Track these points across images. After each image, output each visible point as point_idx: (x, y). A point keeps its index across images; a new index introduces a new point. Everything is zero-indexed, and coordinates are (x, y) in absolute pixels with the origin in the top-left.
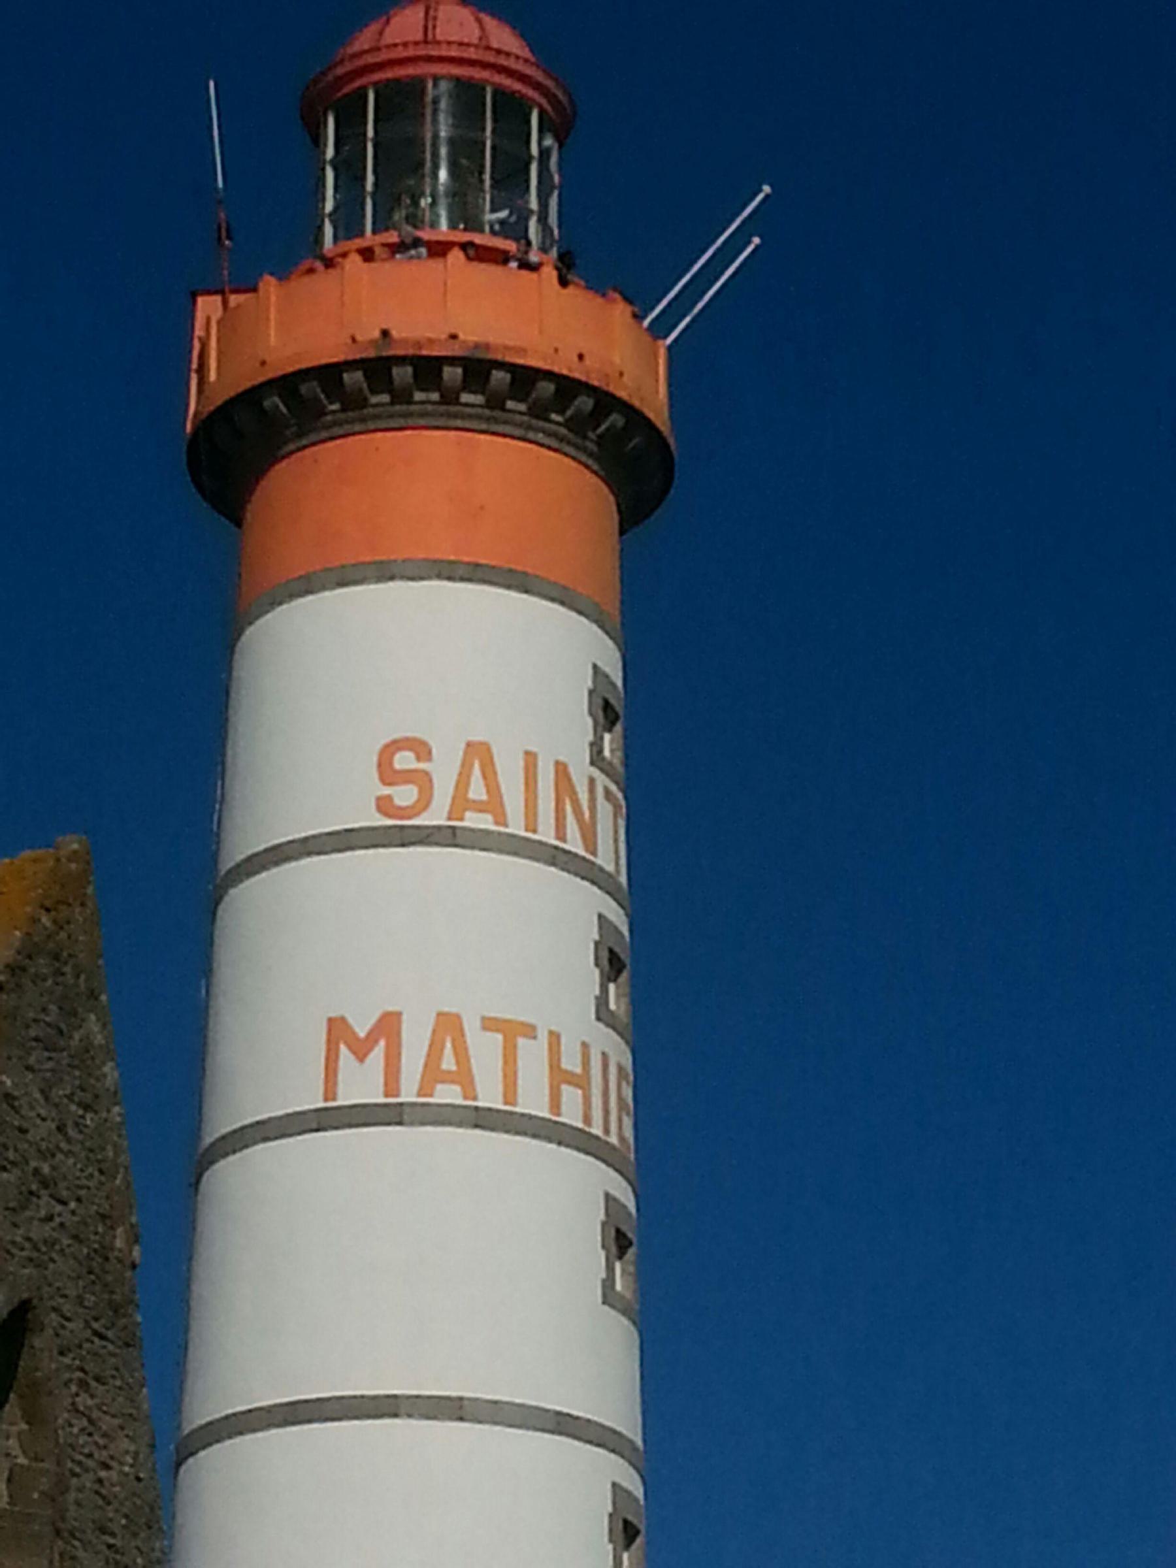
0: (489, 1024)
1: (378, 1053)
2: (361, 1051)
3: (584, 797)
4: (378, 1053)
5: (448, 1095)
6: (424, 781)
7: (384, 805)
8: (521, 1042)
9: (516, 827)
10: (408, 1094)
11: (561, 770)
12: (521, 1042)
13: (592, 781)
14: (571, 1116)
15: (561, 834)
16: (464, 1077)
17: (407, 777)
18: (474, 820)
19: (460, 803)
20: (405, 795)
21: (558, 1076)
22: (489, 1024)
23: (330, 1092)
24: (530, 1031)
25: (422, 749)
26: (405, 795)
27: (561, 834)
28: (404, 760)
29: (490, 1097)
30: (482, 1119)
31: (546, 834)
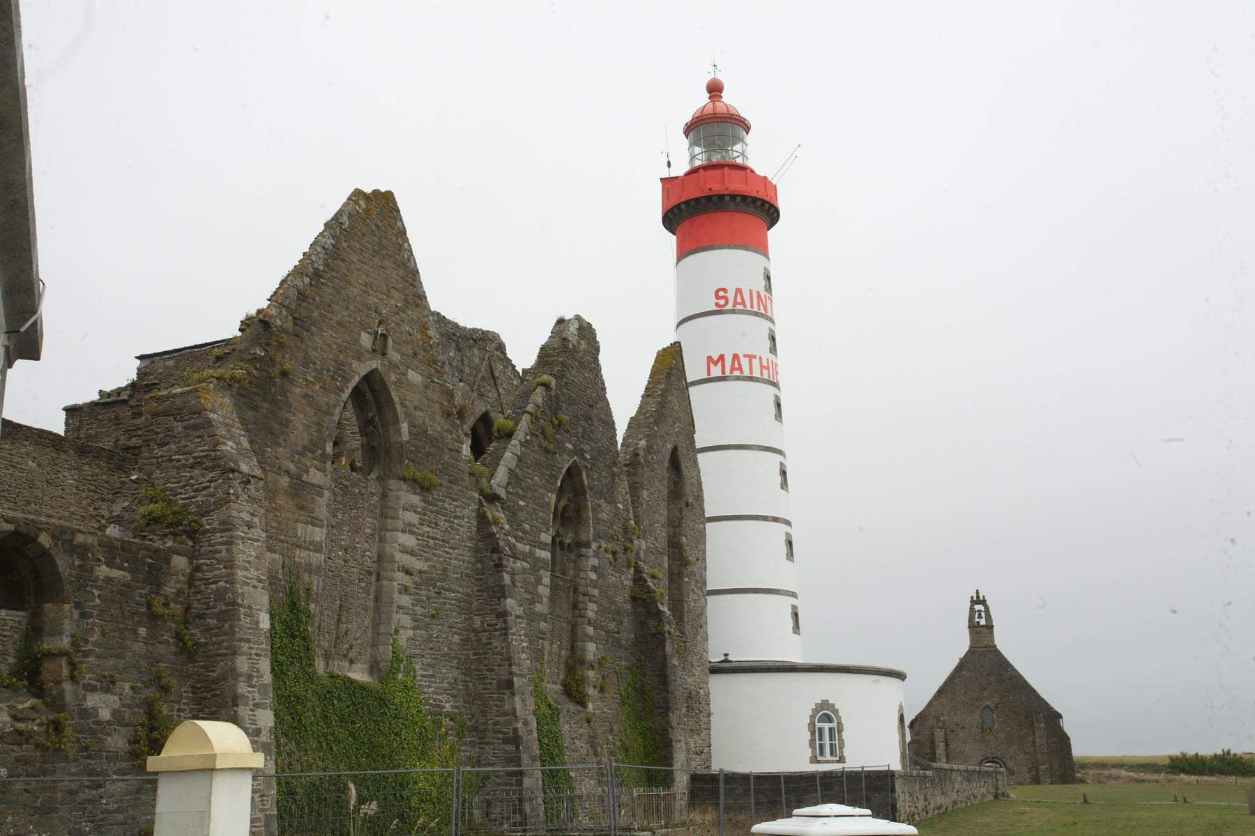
0: (745, 356)
1: (720, 364)
2: (716, 363)
3: (763, 299)
4: (720, 364)
5: (737, 373)
6: (726, 299)
8: (753, 360)
9: (749, 308)
10: (727, 373)
11: (758, 293)
12: (753, 360)
13: (765, 296)
14: (765, 376)
15: (759, 309)
16: (740, 369)
17: (722, 297)
19: (735, 303)
20: (722, 302)
21: (762, 367)
22: (745, 356)
23: (709, 374)
24: (755, 357)
25: (724, 290)
26: (722, 302)
27: (759, 309)
28: (721, 294)
29: (746, 373)
31: (756, 309)
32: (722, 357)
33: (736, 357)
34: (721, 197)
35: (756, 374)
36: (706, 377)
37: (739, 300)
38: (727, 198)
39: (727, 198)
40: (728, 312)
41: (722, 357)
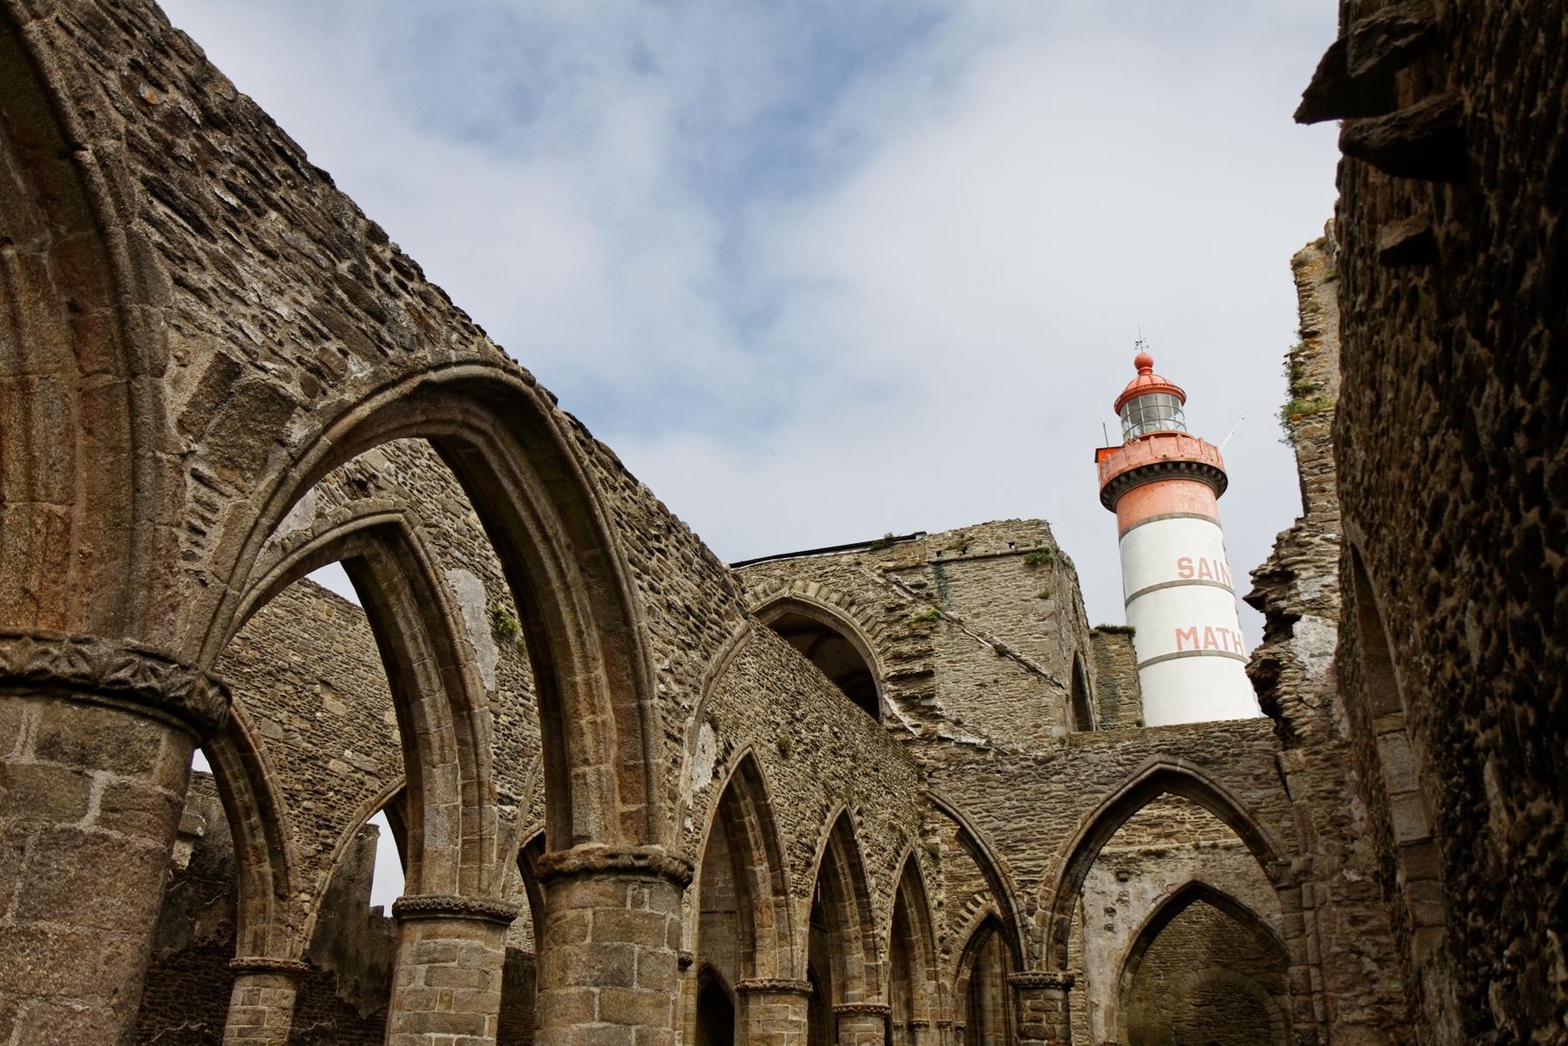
0: (1218, 629)
2: (1187, 638)
5: (1212, 648)
6: (1191, 568)
7: (1181, 574)
10: (1201, 648)
16: (1215, 643)
18: (1206, 578)
19: (1201, 574)
22: (1218, 629)
23: (1180, 647)
25: (1189, 561)
26: (1187, 572)
28: (1185, 563)
29: (1222, 648)
30: (1221, 654)
32: (1193, 631)
33: (1208, 630)
34: (1176, 464)
35: (1231, 650)
36: (1175, 650)
37: (1204, 571)
38: (1183, 466)
39: (1183, 466)
40: (1194, 583)
41: (1193, 631)
